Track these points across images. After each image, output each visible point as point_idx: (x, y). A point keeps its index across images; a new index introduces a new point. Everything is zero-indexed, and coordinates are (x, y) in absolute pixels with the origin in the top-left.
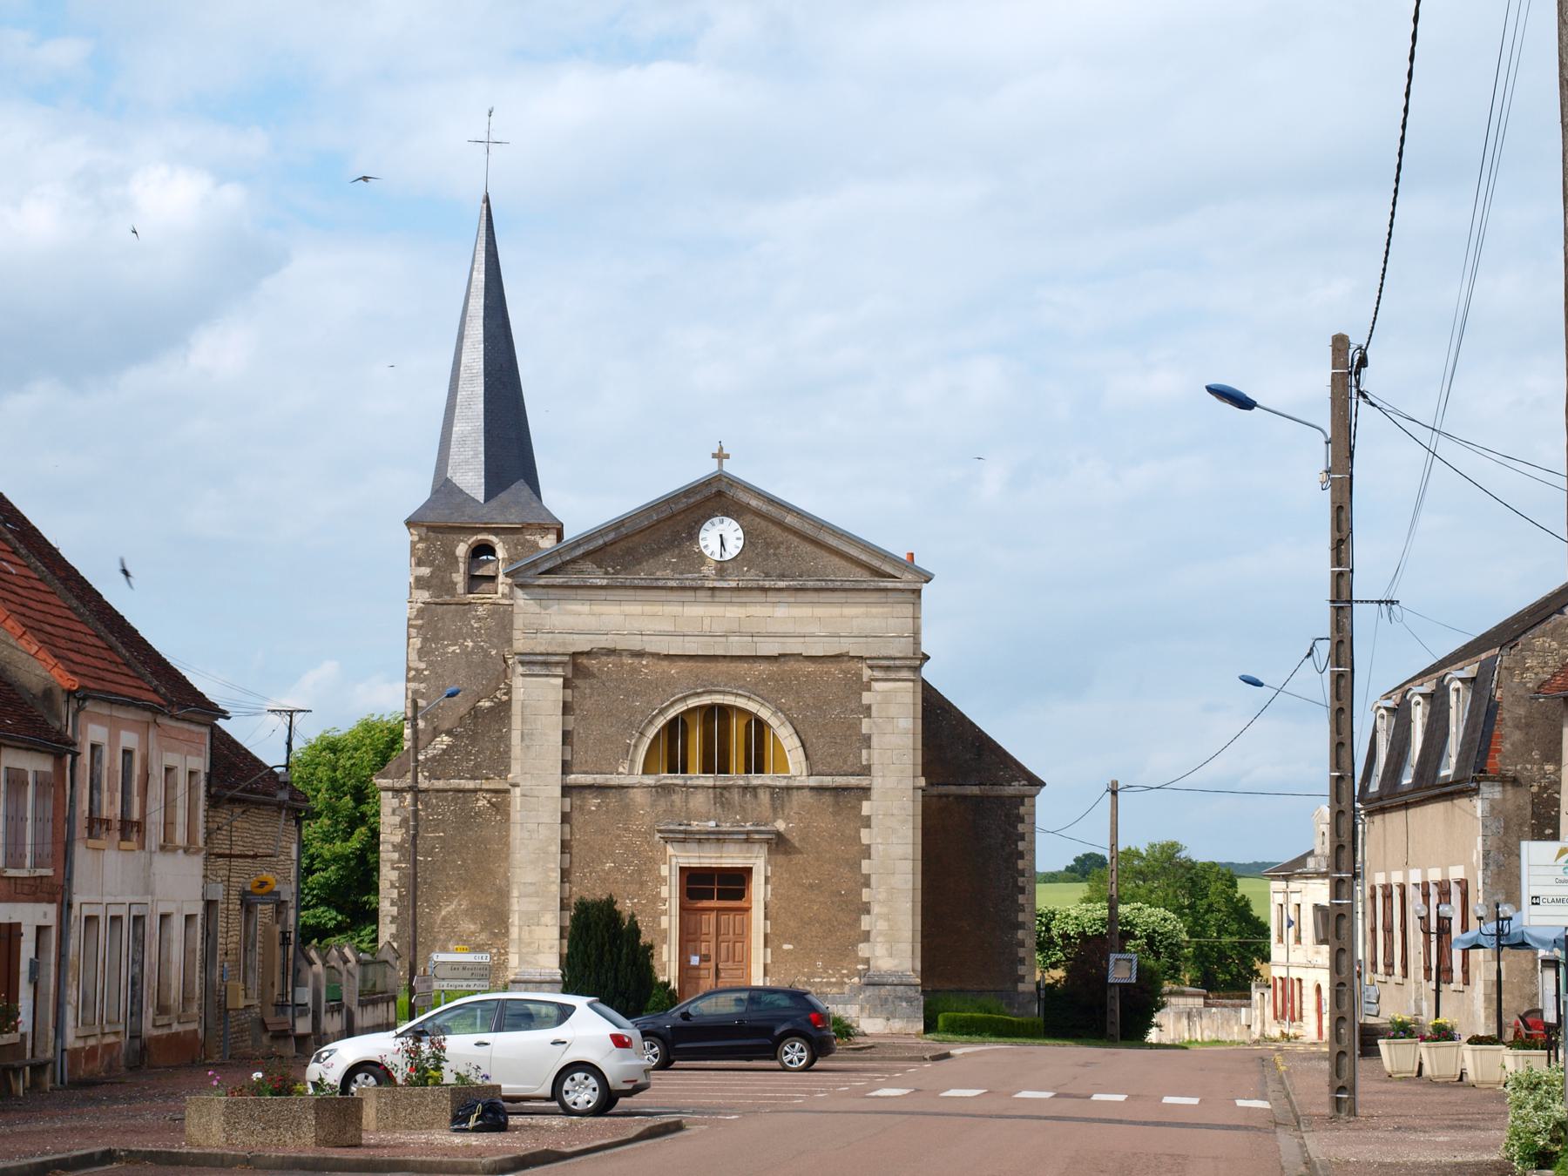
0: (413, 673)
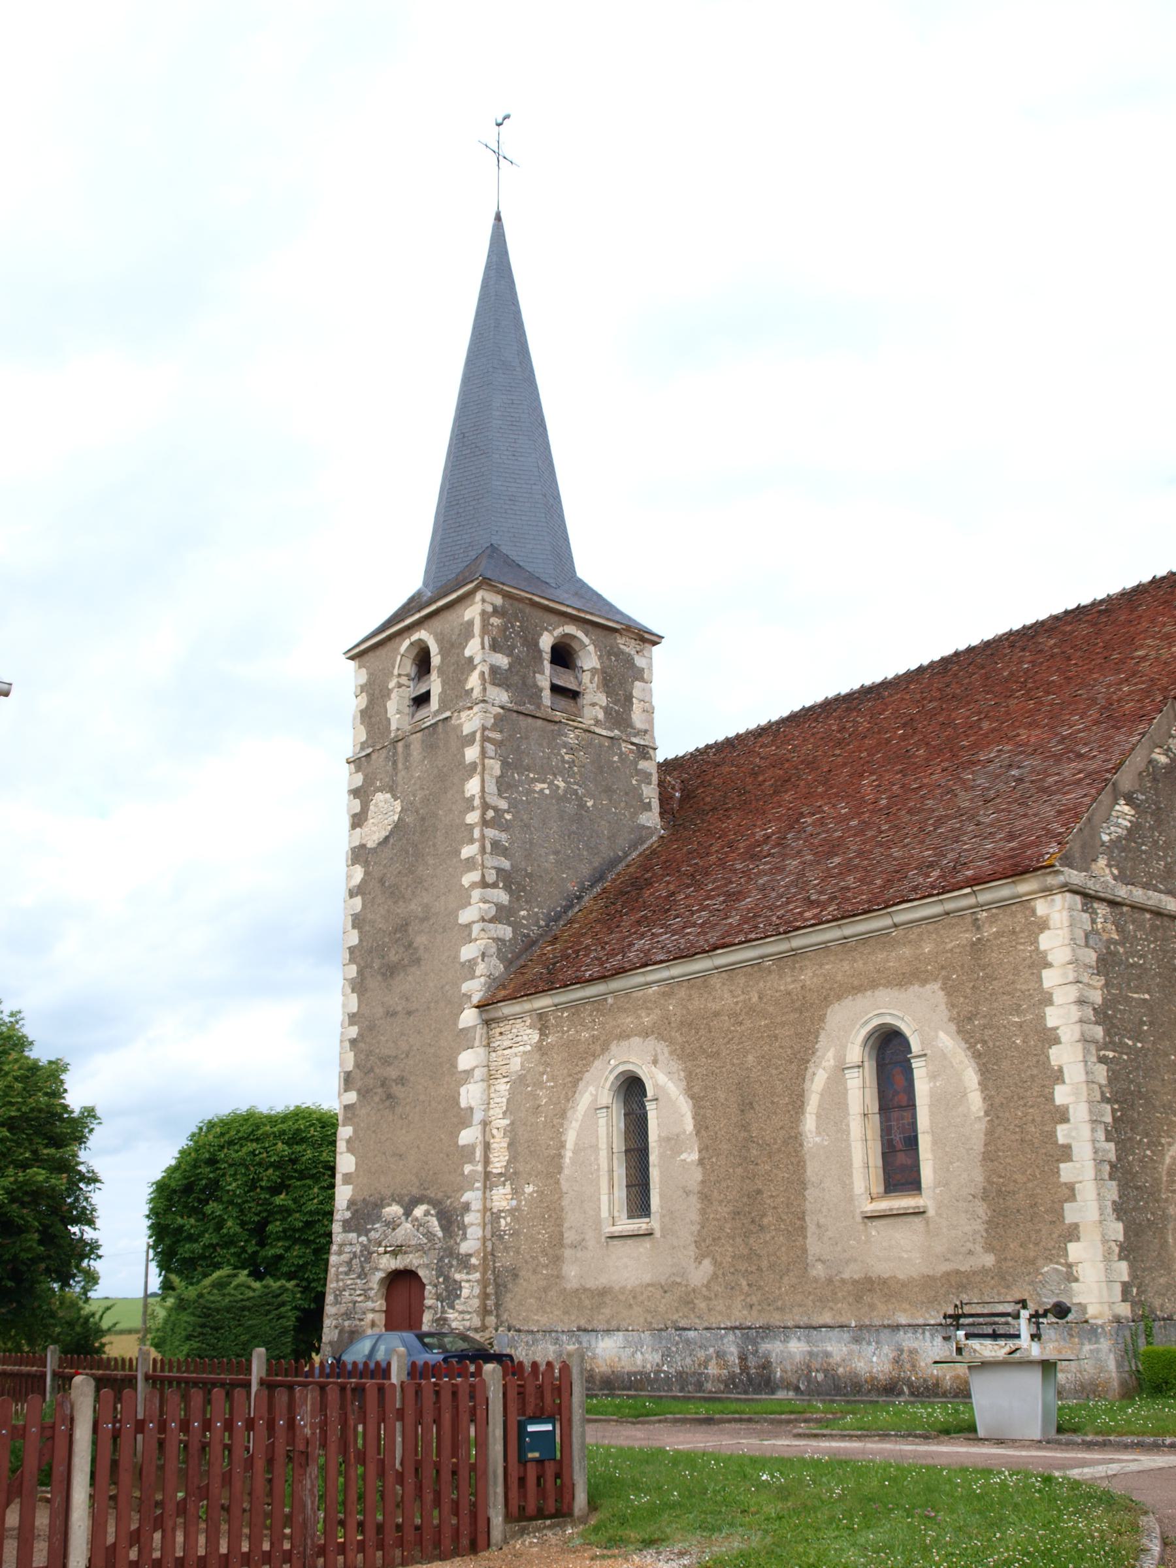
0: (490, 814)
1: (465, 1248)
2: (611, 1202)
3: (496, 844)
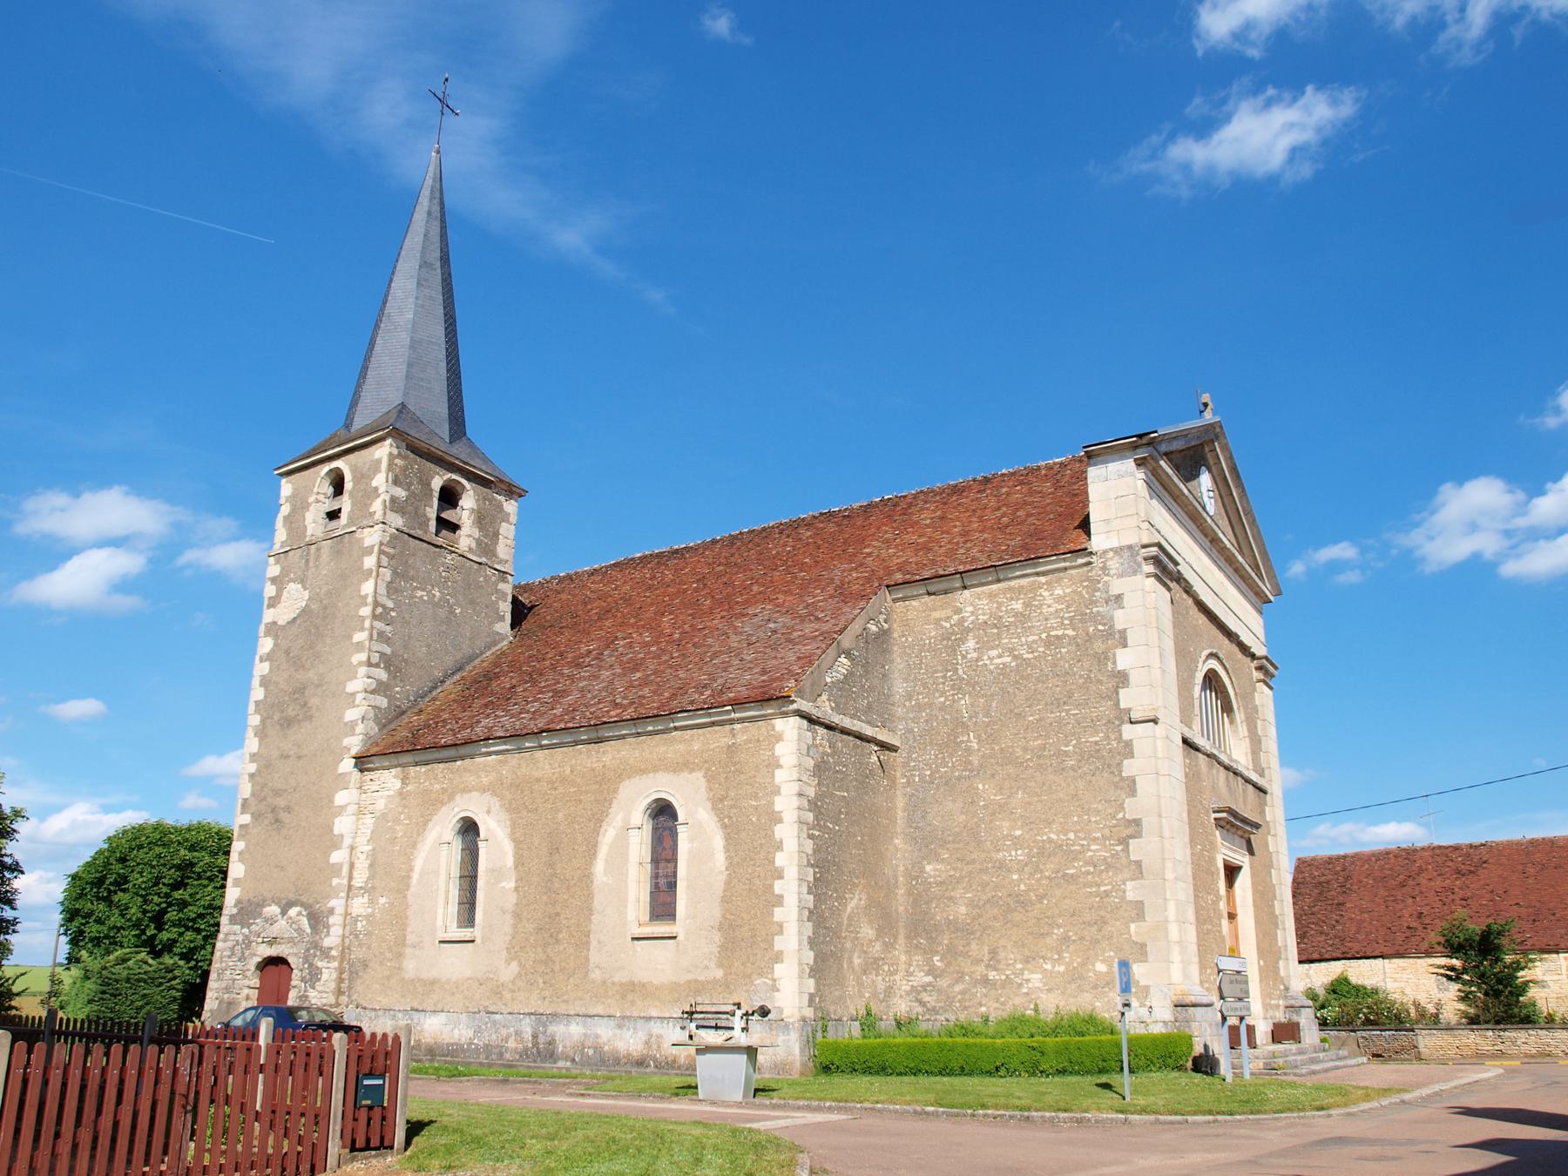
0: (380, 610)
1: (327, 942)
2: (445, 915)
3: (381, 634)
